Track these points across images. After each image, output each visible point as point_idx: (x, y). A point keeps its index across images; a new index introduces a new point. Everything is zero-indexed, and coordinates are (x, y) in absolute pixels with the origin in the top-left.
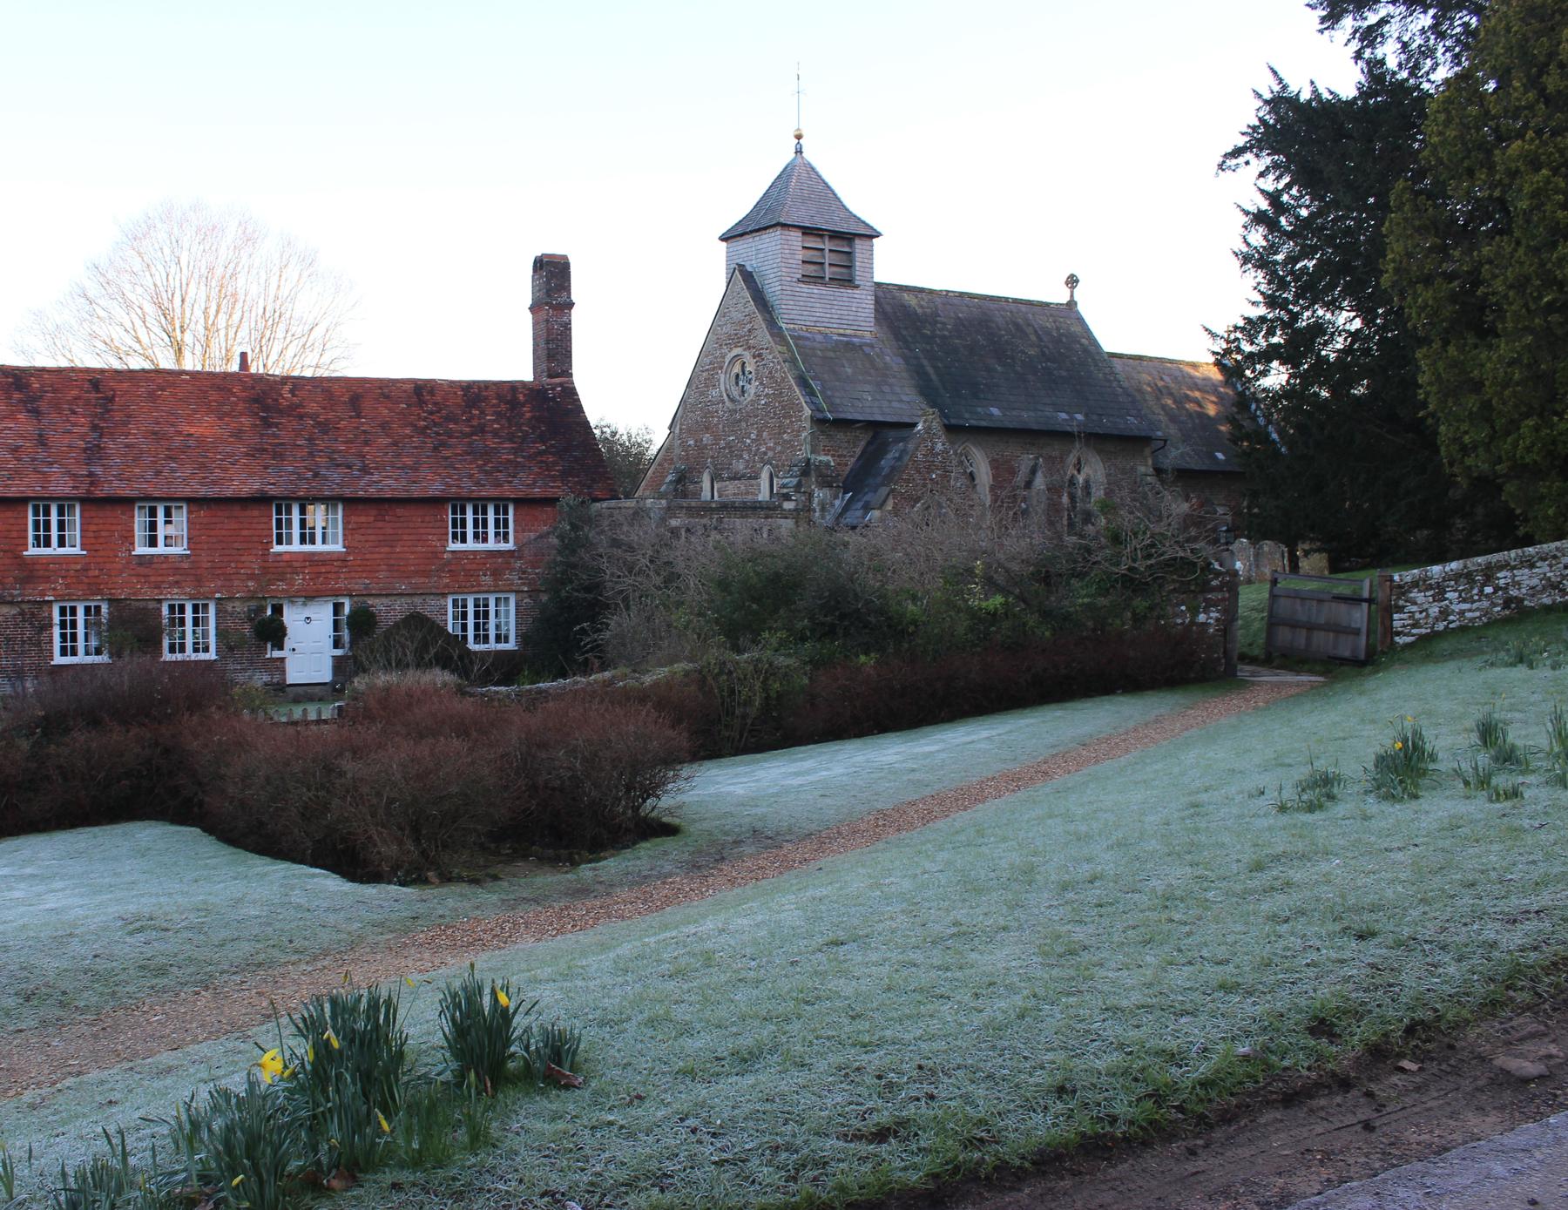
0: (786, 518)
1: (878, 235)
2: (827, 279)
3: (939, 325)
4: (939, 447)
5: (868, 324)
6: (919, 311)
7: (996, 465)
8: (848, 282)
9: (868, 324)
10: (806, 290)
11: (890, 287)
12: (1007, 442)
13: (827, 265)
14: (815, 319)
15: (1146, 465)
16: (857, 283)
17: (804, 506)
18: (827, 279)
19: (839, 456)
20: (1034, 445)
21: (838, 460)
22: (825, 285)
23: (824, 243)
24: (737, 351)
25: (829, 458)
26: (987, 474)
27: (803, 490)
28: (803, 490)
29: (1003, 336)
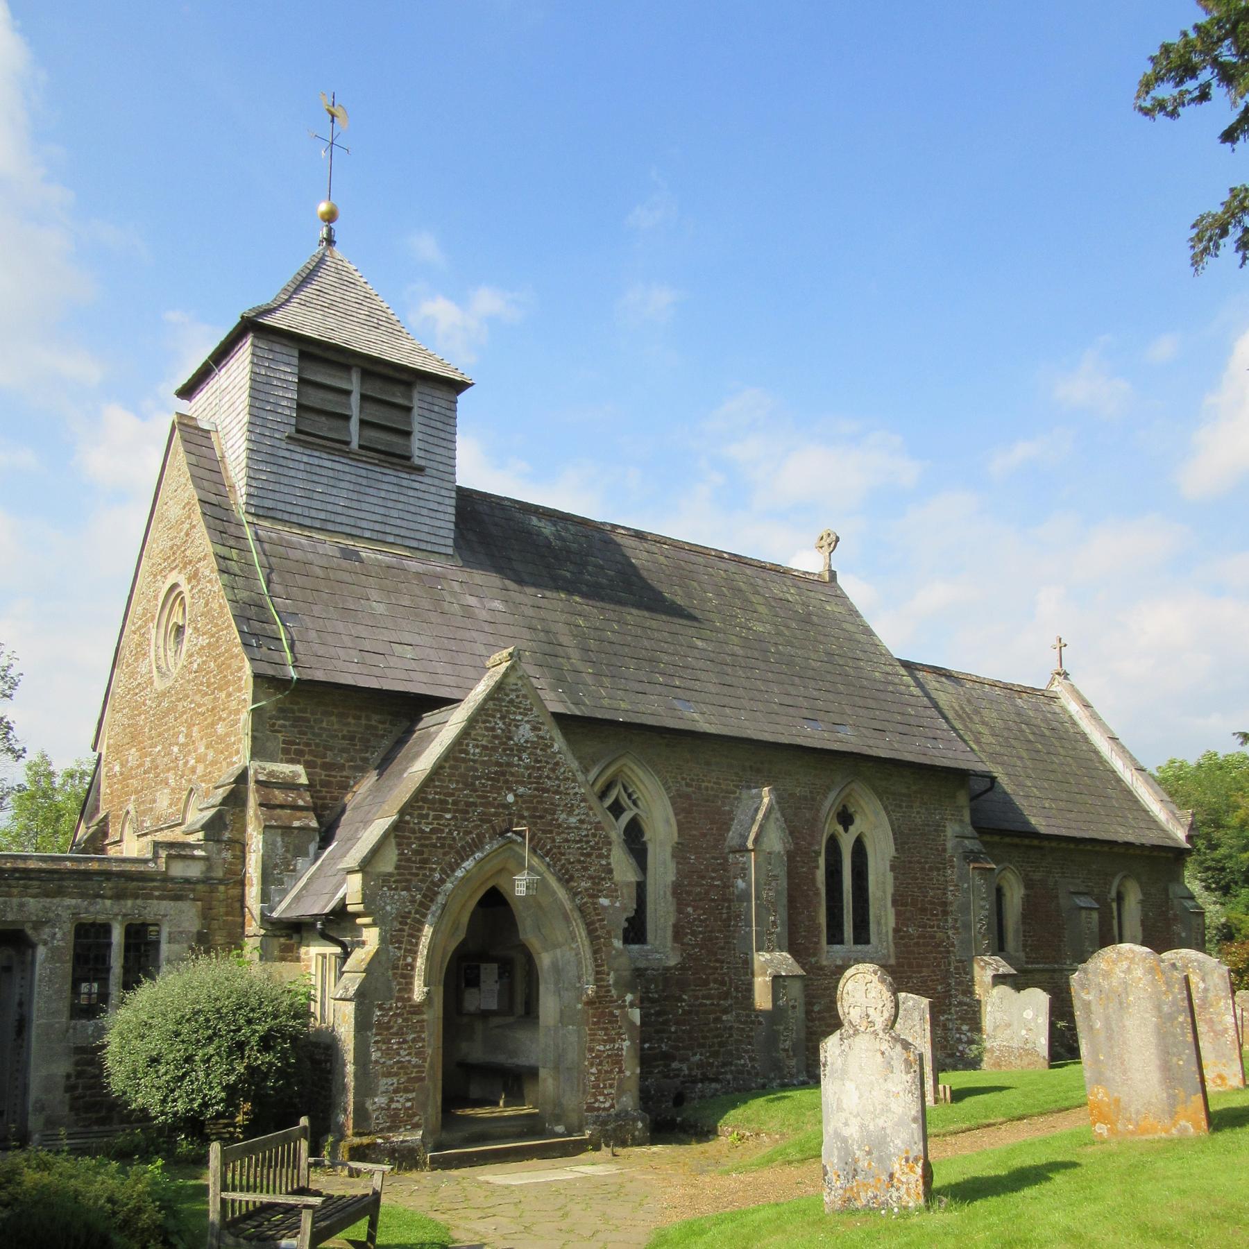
0: (177, 898)
1: (458, 386)
2: (355, 445)
3: (590, 568)
4: (524, 732)
5: (442, 541)
6: (556, 543)
7: (684, 807)
8: (401, 461)
9: (442, 541)
10: (305, 459)
11: (506, 503)
12: (708, 764)
13: (354, 425)
14: (322, 515)
15: (961, 821)
16: (417, 461)
17: (230, 872)
18: (355, 445)
19: (327, 767)
20: (758, 771)
21: (322, 774)
22: (347, 454)
23: (351, 382)
24: (173, 578)
25: (300, 769)
26: (668, 821)
27: (227, 835)
28: (227, 835)
29: (710, 600)
